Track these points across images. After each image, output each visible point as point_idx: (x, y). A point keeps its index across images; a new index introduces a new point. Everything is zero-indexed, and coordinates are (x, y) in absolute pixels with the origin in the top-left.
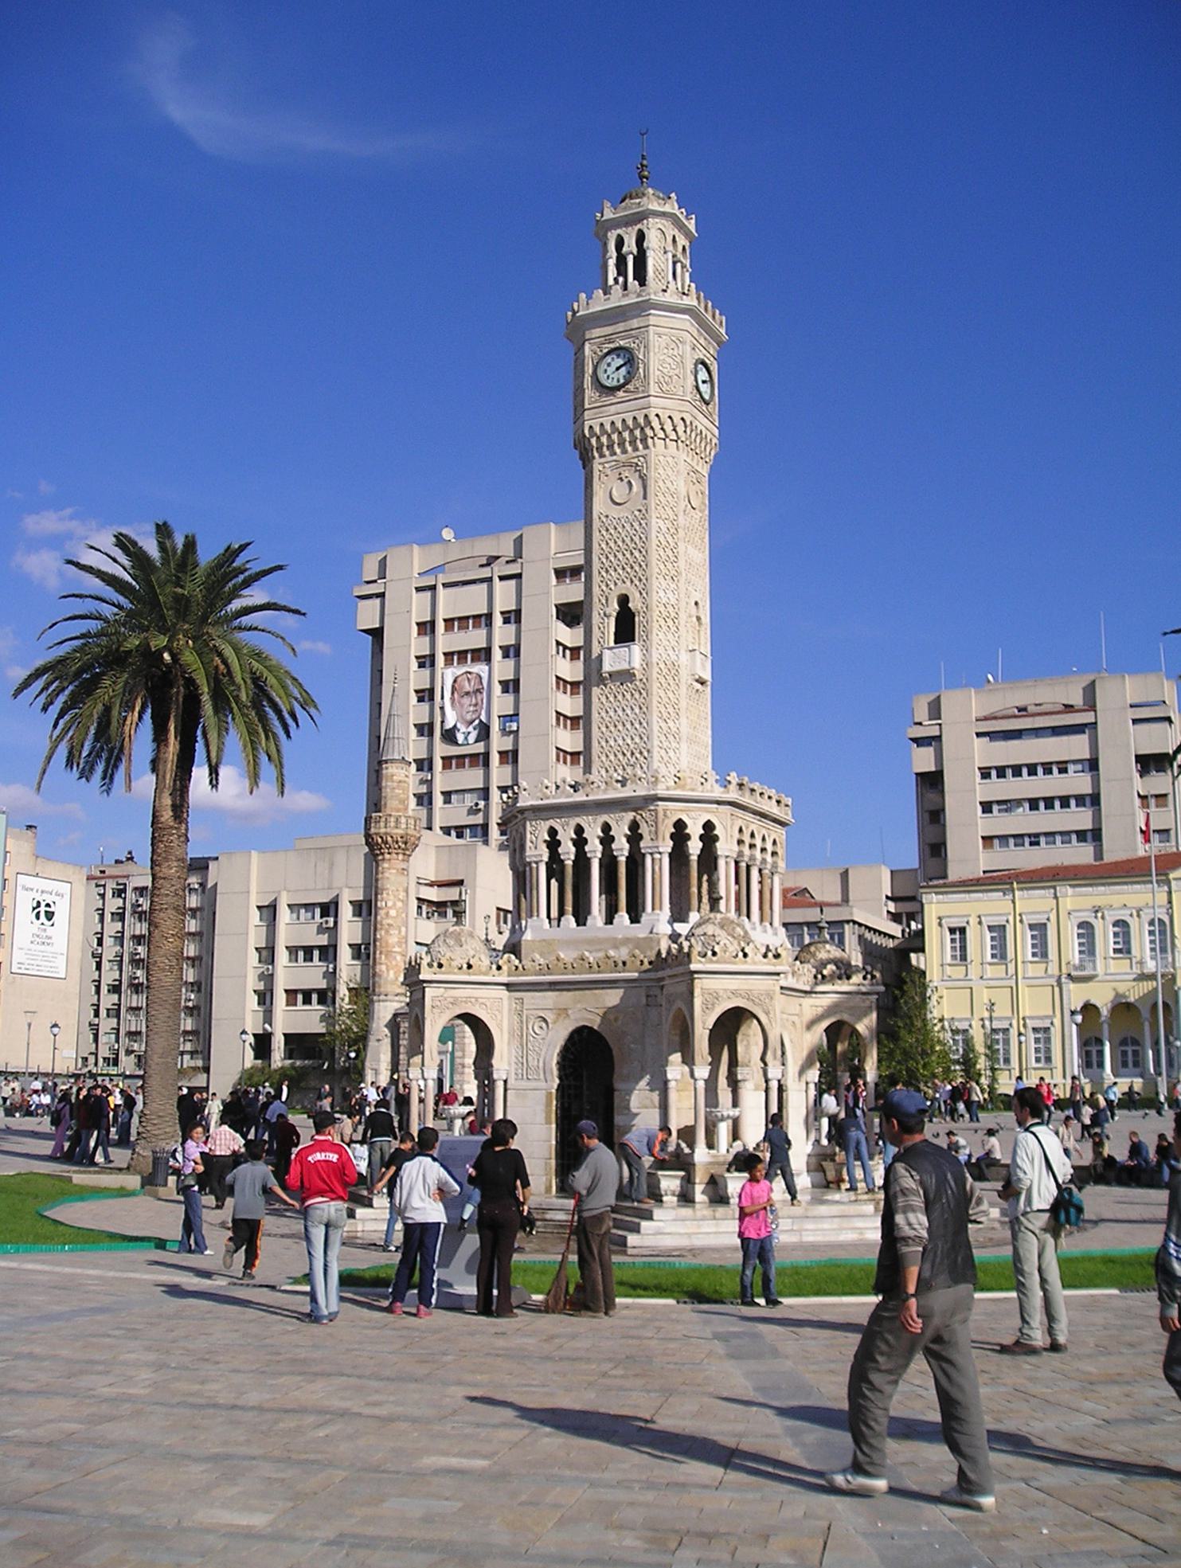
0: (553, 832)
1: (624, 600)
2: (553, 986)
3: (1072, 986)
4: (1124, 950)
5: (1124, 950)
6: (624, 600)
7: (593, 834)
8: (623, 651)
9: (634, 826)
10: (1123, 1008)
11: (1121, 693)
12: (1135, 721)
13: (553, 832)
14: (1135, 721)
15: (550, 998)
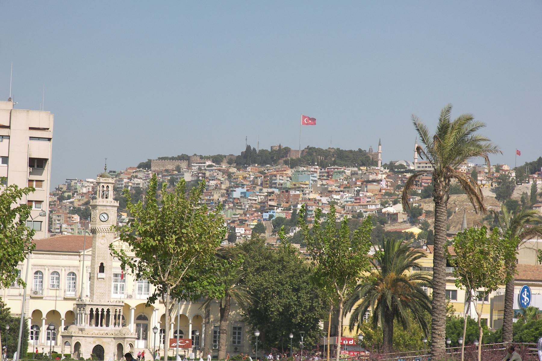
0: (92, 309)
1: (102, 264)
2: (93, 337)
3: (32, 301)
4: (56, 287)
5: (56, 287)
6: (102, 264)
7: (100, 310)
8: (101, 274)
9: (108, 310)
10: (54, 313)
11: (22, 121)
12: (31, 138)
13: (92, 309)
14: (31, 138)
15: (92, 339)
